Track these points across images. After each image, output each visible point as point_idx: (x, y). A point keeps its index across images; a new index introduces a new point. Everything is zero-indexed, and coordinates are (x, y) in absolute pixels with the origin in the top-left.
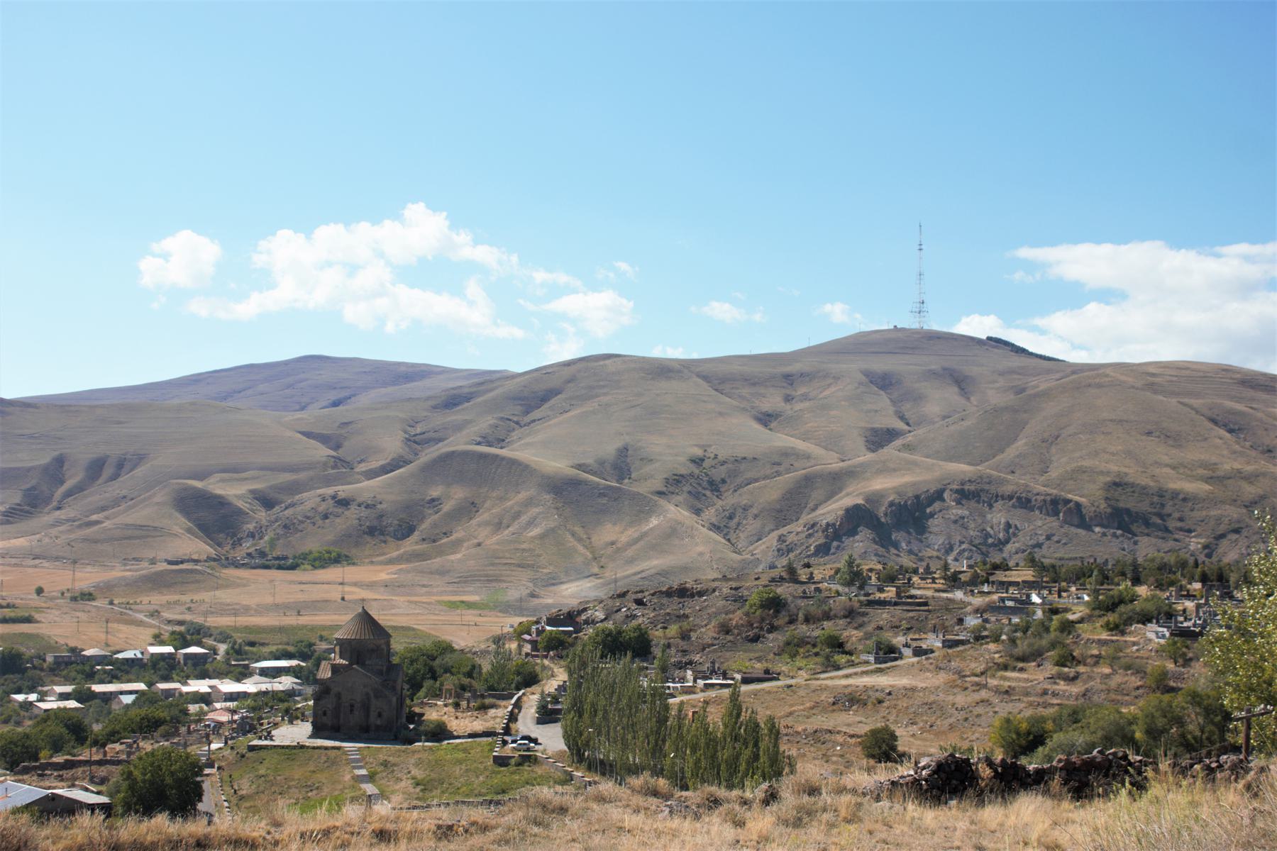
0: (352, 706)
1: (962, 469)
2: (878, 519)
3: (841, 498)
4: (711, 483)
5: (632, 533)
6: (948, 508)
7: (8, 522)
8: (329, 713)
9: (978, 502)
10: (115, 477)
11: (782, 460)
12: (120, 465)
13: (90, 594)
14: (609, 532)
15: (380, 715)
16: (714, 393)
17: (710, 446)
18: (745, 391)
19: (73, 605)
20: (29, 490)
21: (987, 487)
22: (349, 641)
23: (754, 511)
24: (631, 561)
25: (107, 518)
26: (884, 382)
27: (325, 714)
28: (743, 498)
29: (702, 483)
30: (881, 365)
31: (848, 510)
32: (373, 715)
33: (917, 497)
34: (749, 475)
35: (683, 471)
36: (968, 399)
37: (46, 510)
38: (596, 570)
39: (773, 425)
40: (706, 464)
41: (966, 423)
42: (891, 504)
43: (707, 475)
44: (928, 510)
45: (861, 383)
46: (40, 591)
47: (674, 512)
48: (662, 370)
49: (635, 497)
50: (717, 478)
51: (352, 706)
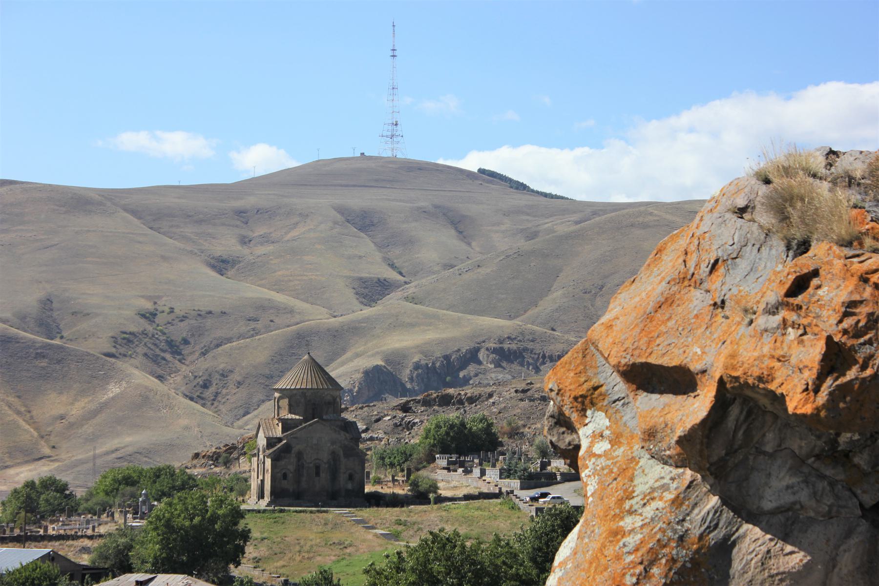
0: (318, 468)
1: (494, 325)
2: (403, 385)
3: (351, 360)
4: (170, 343)
5: (77, 410)
6: (485, 372)
8: (290, 475)
9: (522, 365)
11: (258, 315)
14: (55, 404)
16: (150, 231)
17: (159, 297)
18: (189, 230)
21: (530, 346)
22: (303, 392)
23: (236, 377)
24: (92, 439)
26: (365, 222)
27: (285, 476)
28: (219, 360)
29: (162, 342)
30: (359, 200)
31: (367, 373)
33: (447, 357)
34: (219, 333)
35: (133, 328)
36: (469, 244)
38: (47, 451)
39: (231, 273)
40: (161, 319)
41: (483, 271)
42: (417, 366)
43: (164, 334)
44: (461, 374)
45: (335, 223)
47: (136, 376)
48: (78, 202)
49: (82, 358)
50: (177, 338)
51: (318, 468)
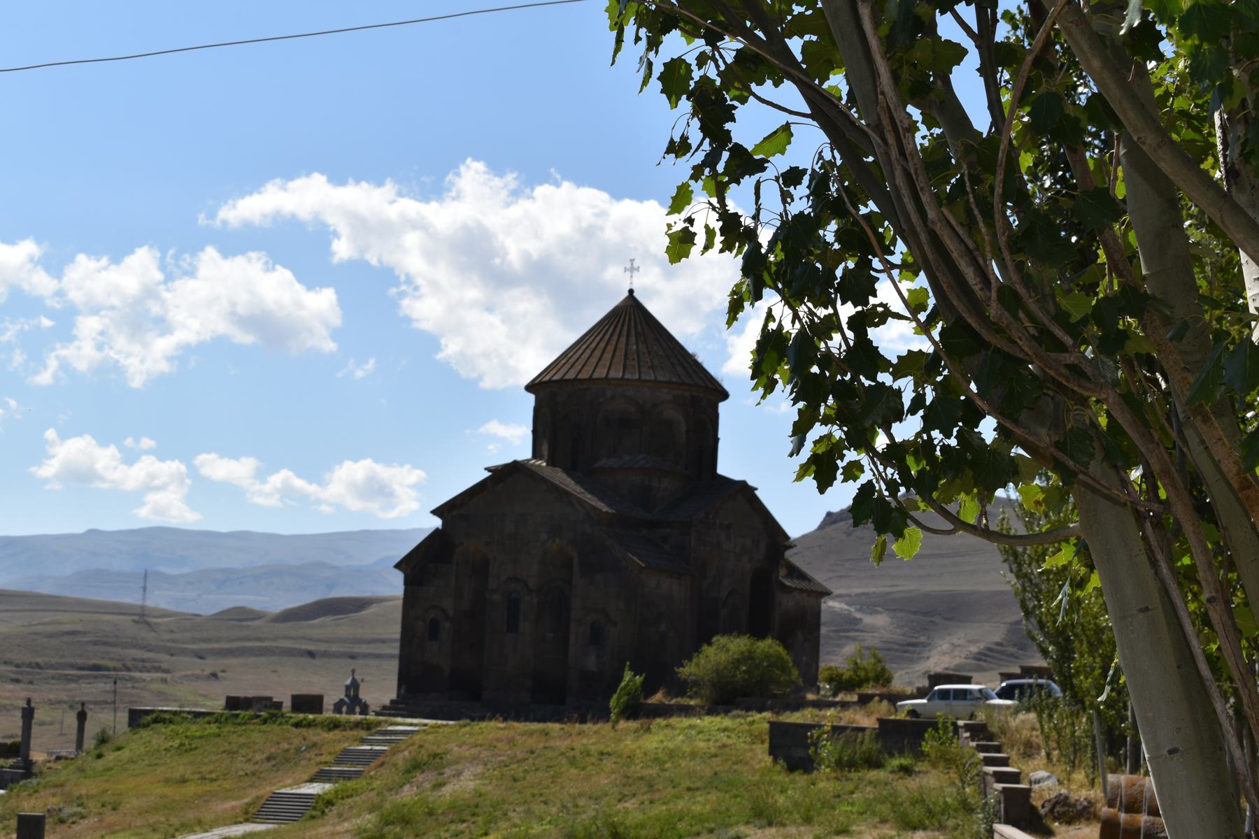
15: (596, 637)
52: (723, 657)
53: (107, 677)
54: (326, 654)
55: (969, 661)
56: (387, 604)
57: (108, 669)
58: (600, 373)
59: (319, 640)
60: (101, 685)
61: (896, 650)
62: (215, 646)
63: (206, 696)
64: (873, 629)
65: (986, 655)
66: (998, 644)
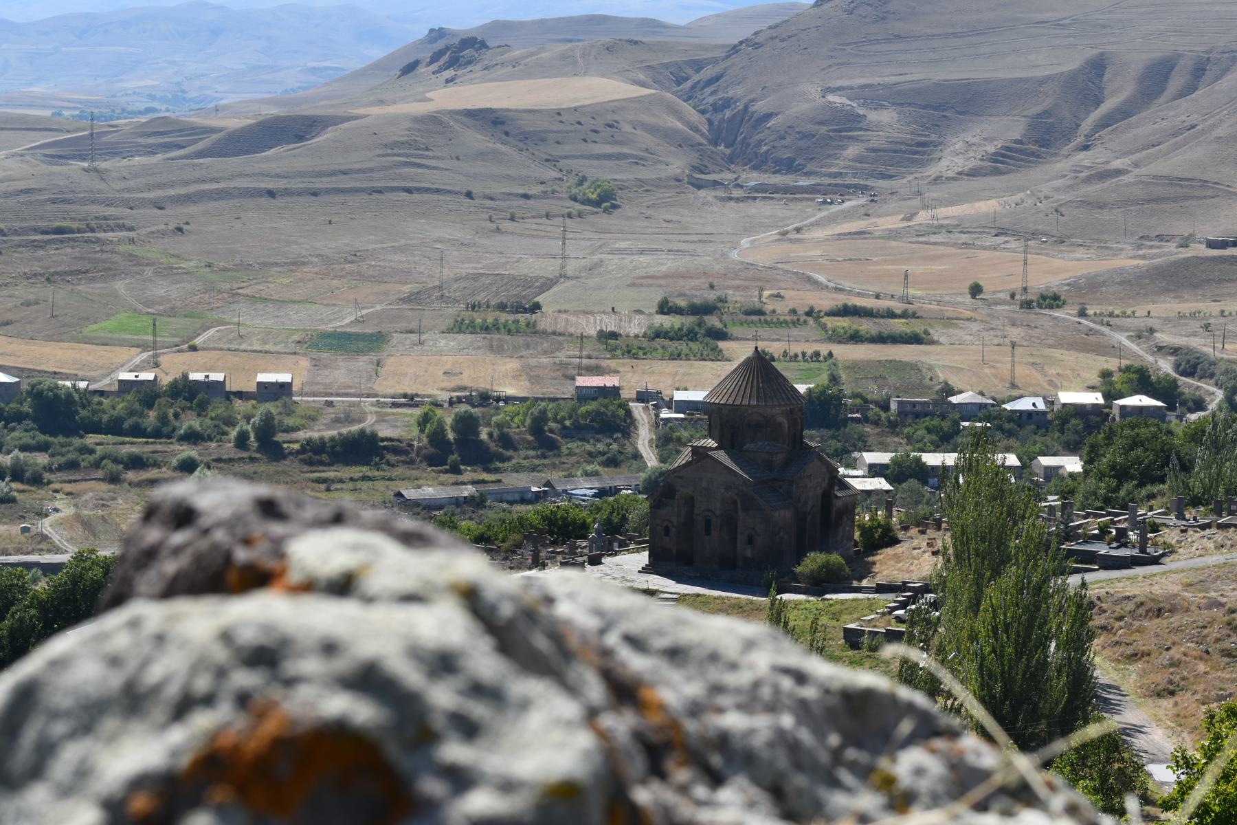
0: (708, 523)
7: (997, 172)
10: (1190, 89)
12: (1199, 72)
13: (1056, 298)
15: (750, 540)
19: (1022, 315)
20: (1039, 116)
25: (1136, 165)
27: (667, 531)
32: (741, 539)
37: (1065, 151)
46: (976, 290)
51: (708, 523)
52: (815, 566)
53: (74, 240)
54: (286, 192)
55: (984, 163)
56: (346, 125)
57: (71, 231)
58: (746, 402)
59: (278, 176)
60: (70, 250)
61: (905, 152)
62: (172, 192)
63: (177, 256)
64: (879, 127)
65: (1004, 156)
66: (1017, 142)
